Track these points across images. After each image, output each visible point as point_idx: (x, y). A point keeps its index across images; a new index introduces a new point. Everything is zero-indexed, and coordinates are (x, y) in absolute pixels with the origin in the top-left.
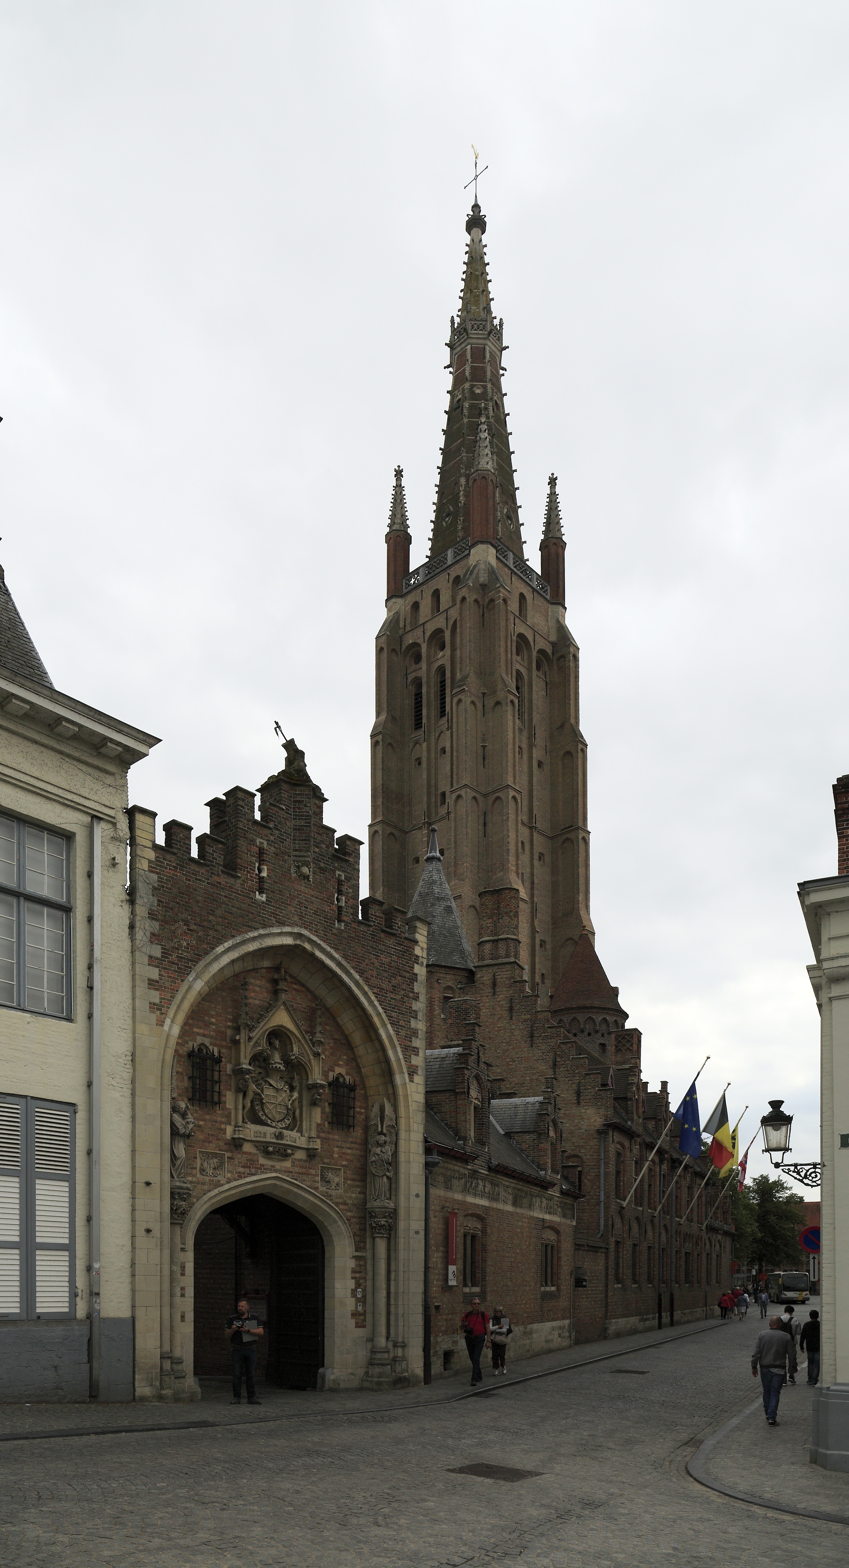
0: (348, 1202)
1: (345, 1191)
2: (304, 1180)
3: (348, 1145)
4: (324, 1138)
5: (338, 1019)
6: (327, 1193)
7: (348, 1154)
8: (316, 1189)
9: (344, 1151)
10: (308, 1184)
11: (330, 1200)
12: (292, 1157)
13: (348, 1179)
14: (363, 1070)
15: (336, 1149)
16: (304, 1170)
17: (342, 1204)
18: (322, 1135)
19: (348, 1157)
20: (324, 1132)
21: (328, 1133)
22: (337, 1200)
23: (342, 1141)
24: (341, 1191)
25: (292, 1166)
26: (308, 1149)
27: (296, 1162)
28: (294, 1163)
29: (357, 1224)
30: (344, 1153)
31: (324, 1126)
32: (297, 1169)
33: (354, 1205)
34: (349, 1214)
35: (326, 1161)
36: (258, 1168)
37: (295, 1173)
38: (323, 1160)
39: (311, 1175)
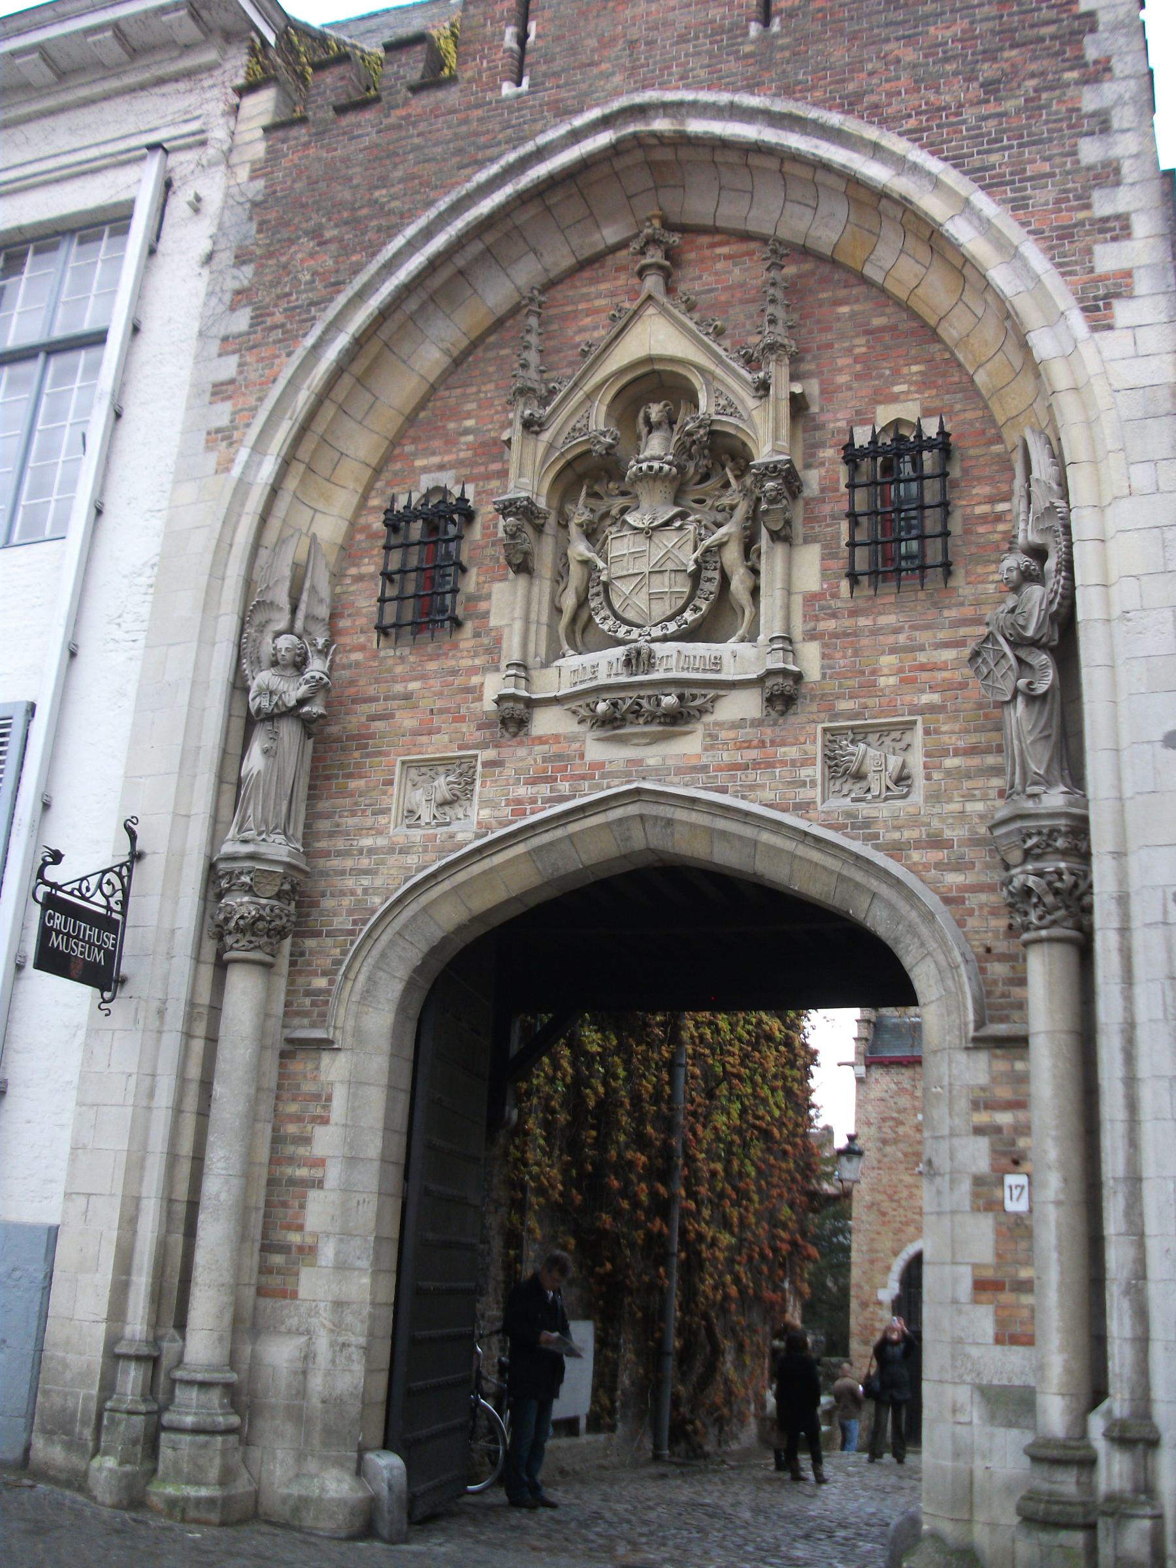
0: (948, 834)
1: (934, 797)
2: (753, 787)
3: (942, 635)
4: (835, 635)
5: (869, 271)
6: (849, 814)
7: (943, 667)
8: (803, 808)
9: (922, 658)
10: (768, 795)
11: (867, 838)
12: (708, 719)
13: (945, 753)
14: (980, 378)
15: (887, 661)
16: (752, 754)
17: (918, 845)
18: (831, 625)
19: (940, 675)
20: (834, 615)
21: (853, 613)
22: (896, 835)
23: (912, 628)
24: (918, 796)
25: (706, 749)
26: (760, 681)
27: (723, 735)
28: (714, 737)
29: (994, 912)
30: (923, 668)
31: (835, 596)
32: (726, 757)
33: (975, 842)
34: (954, 879)
35: (844, 705)
36: (583, 777)
37: (719, 769)
38: (831, 708)
39: (784, 763)
